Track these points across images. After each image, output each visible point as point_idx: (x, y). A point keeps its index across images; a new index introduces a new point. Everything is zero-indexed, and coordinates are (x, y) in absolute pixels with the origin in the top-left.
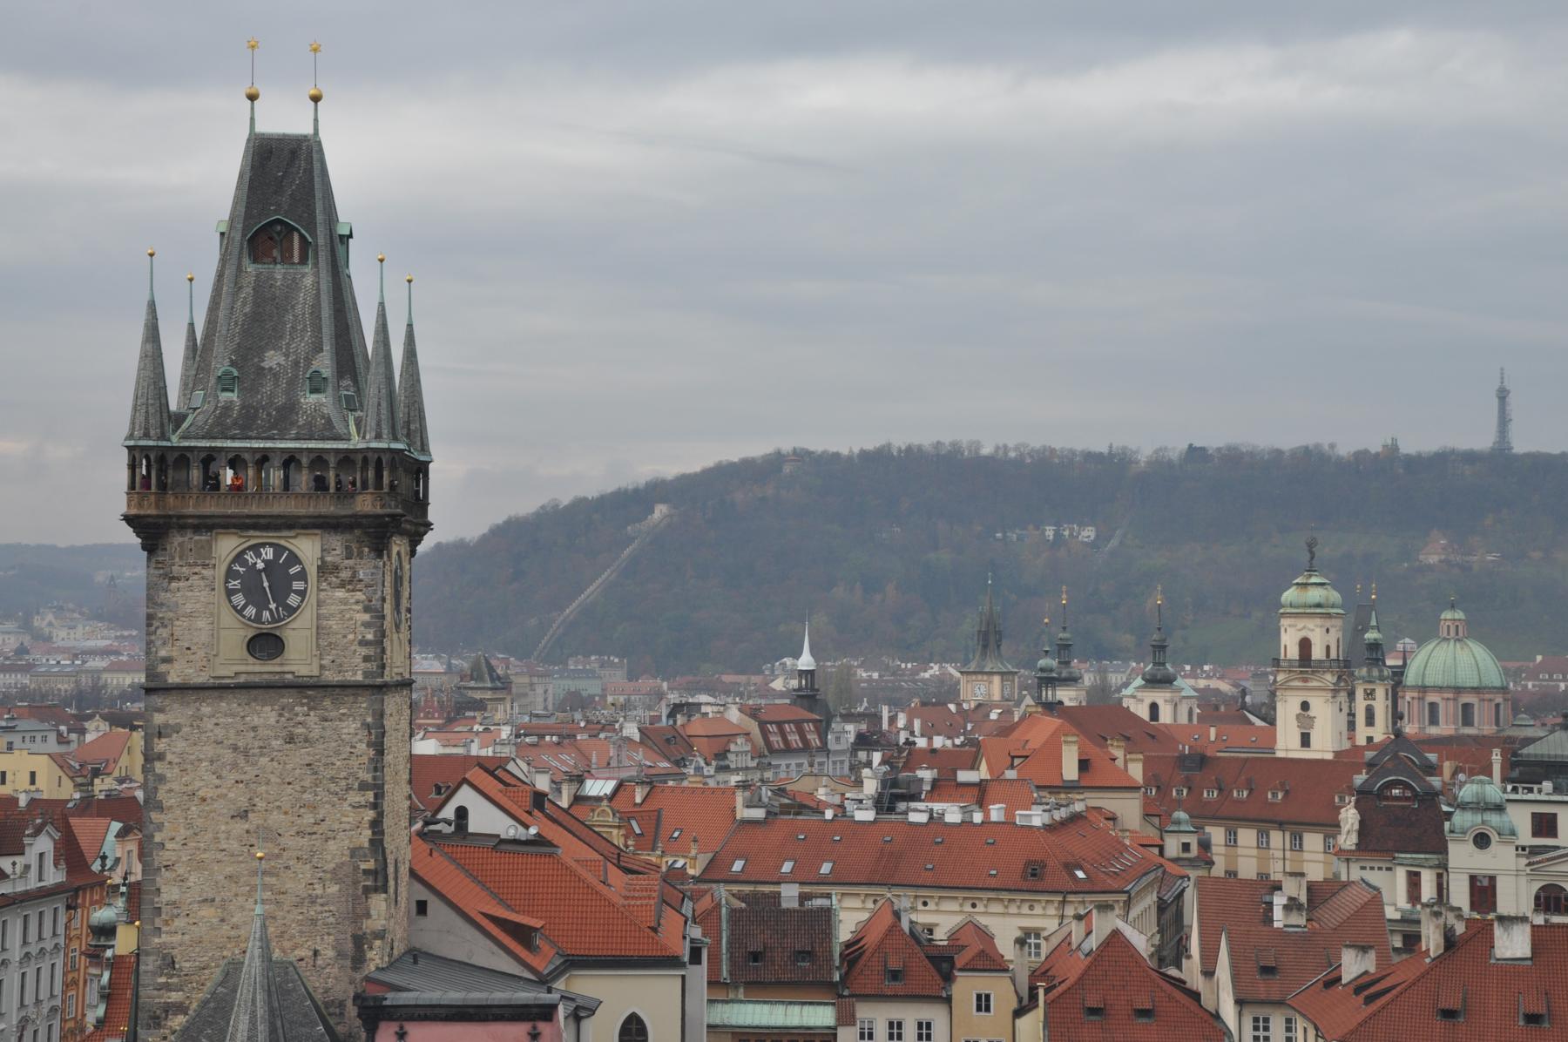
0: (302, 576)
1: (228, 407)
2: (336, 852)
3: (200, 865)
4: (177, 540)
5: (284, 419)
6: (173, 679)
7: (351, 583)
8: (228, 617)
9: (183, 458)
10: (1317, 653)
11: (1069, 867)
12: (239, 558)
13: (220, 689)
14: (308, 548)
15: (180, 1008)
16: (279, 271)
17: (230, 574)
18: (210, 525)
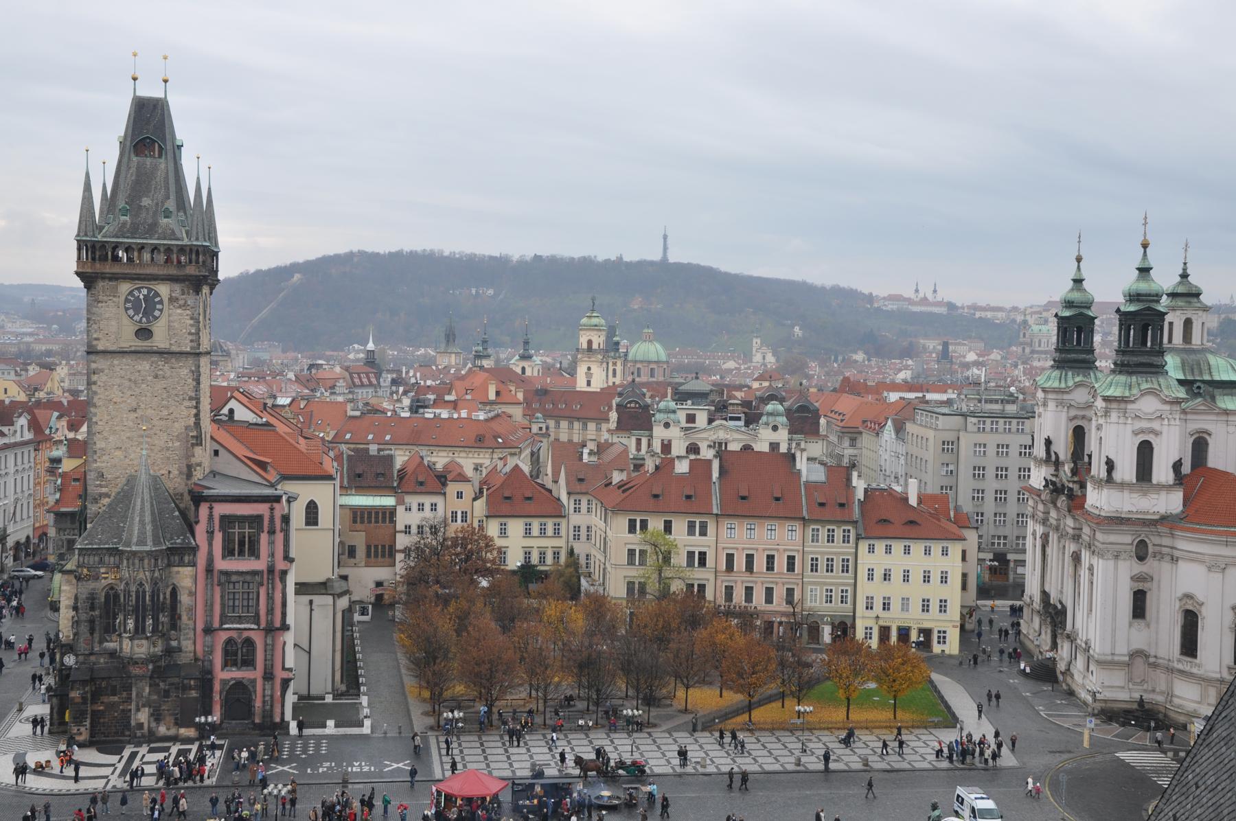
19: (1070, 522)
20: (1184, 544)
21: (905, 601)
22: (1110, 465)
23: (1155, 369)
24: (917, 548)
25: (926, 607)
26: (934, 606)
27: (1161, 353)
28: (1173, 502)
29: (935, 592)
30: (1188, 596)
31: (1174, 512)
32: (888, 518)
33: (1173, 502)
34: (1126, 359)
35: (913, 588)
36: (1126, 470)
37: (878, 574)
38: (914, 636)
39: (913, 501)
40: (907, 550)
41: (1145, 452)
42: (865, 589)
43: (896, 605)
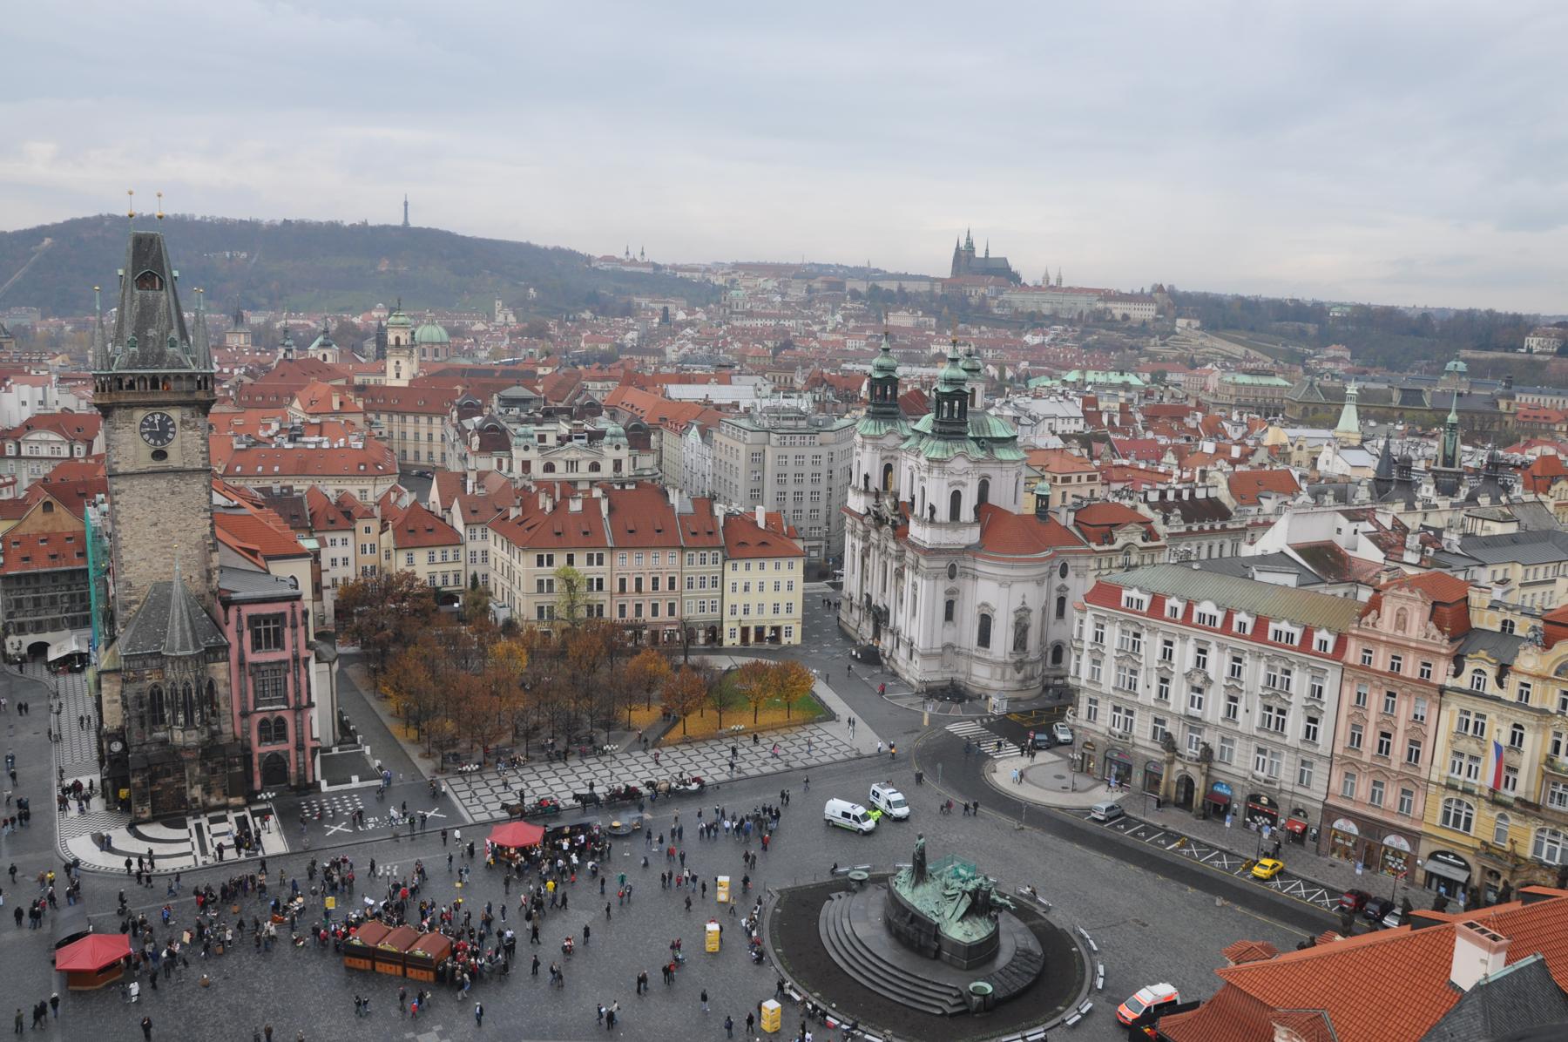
0: (173, 425)
1: (134, 354)
2: (196, 537)
3: (138, 546)
4: (117, 413)
5: (160, 358)
6: (120, 470)
7: (194, 428)
8: (142, 444)
9: (119, 379)
10: (402, 342)
11: (376, 465)
12: (145, 419)
13: (141, 474)
14: (175, 414)
15: (136, 602)
16: (150, 293)
17: (142, 426)
18: (130, 406)
19: (892, 546)
20: (982, 567)
21: (761, 607)
24: (770, 564)
25: (776, 610)
26: (783, 608)
29: (783, 597)
30: (985, 605)
32: (744, 541)
35: (766, 594)
37: (740, 586)
38: (767, 633)
39: (761, 524)
40: (762, 567)
42: (730, 599)
43: (753, 610)
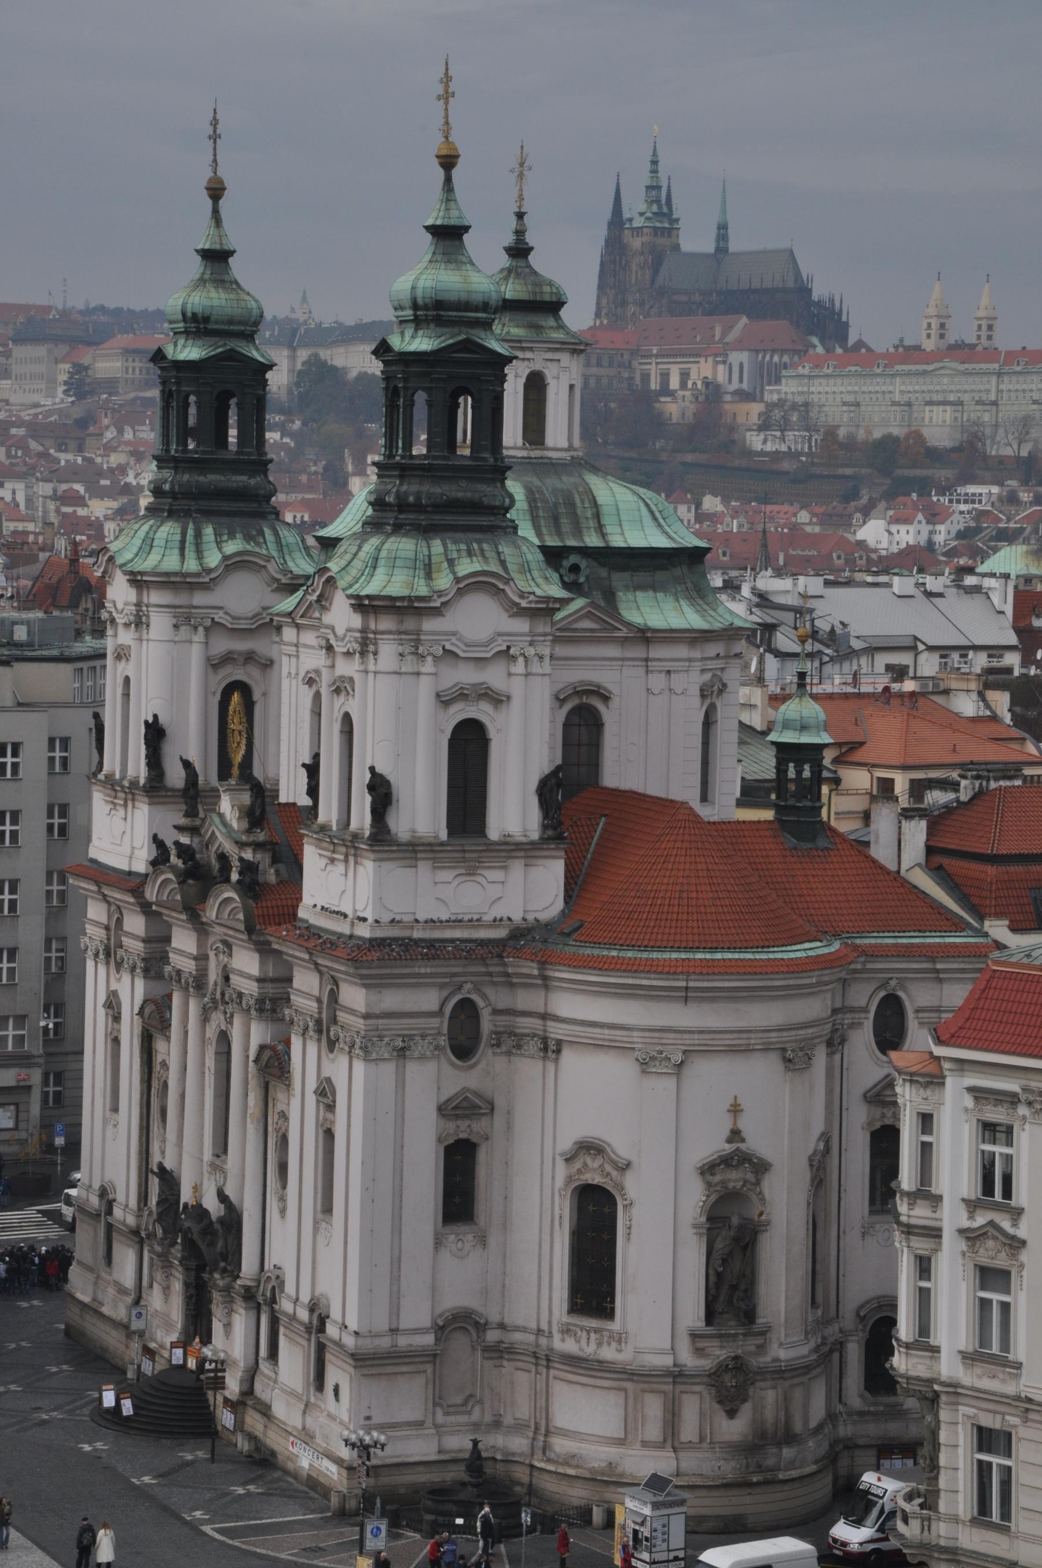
22: (381, 792)
23: (485, 520)
27: (499, 471)
28: (536, 891)
31: (545, 916)
33: (536, 891)
34: (412, 489)
36: (422, 811)
41: (468, 752)
